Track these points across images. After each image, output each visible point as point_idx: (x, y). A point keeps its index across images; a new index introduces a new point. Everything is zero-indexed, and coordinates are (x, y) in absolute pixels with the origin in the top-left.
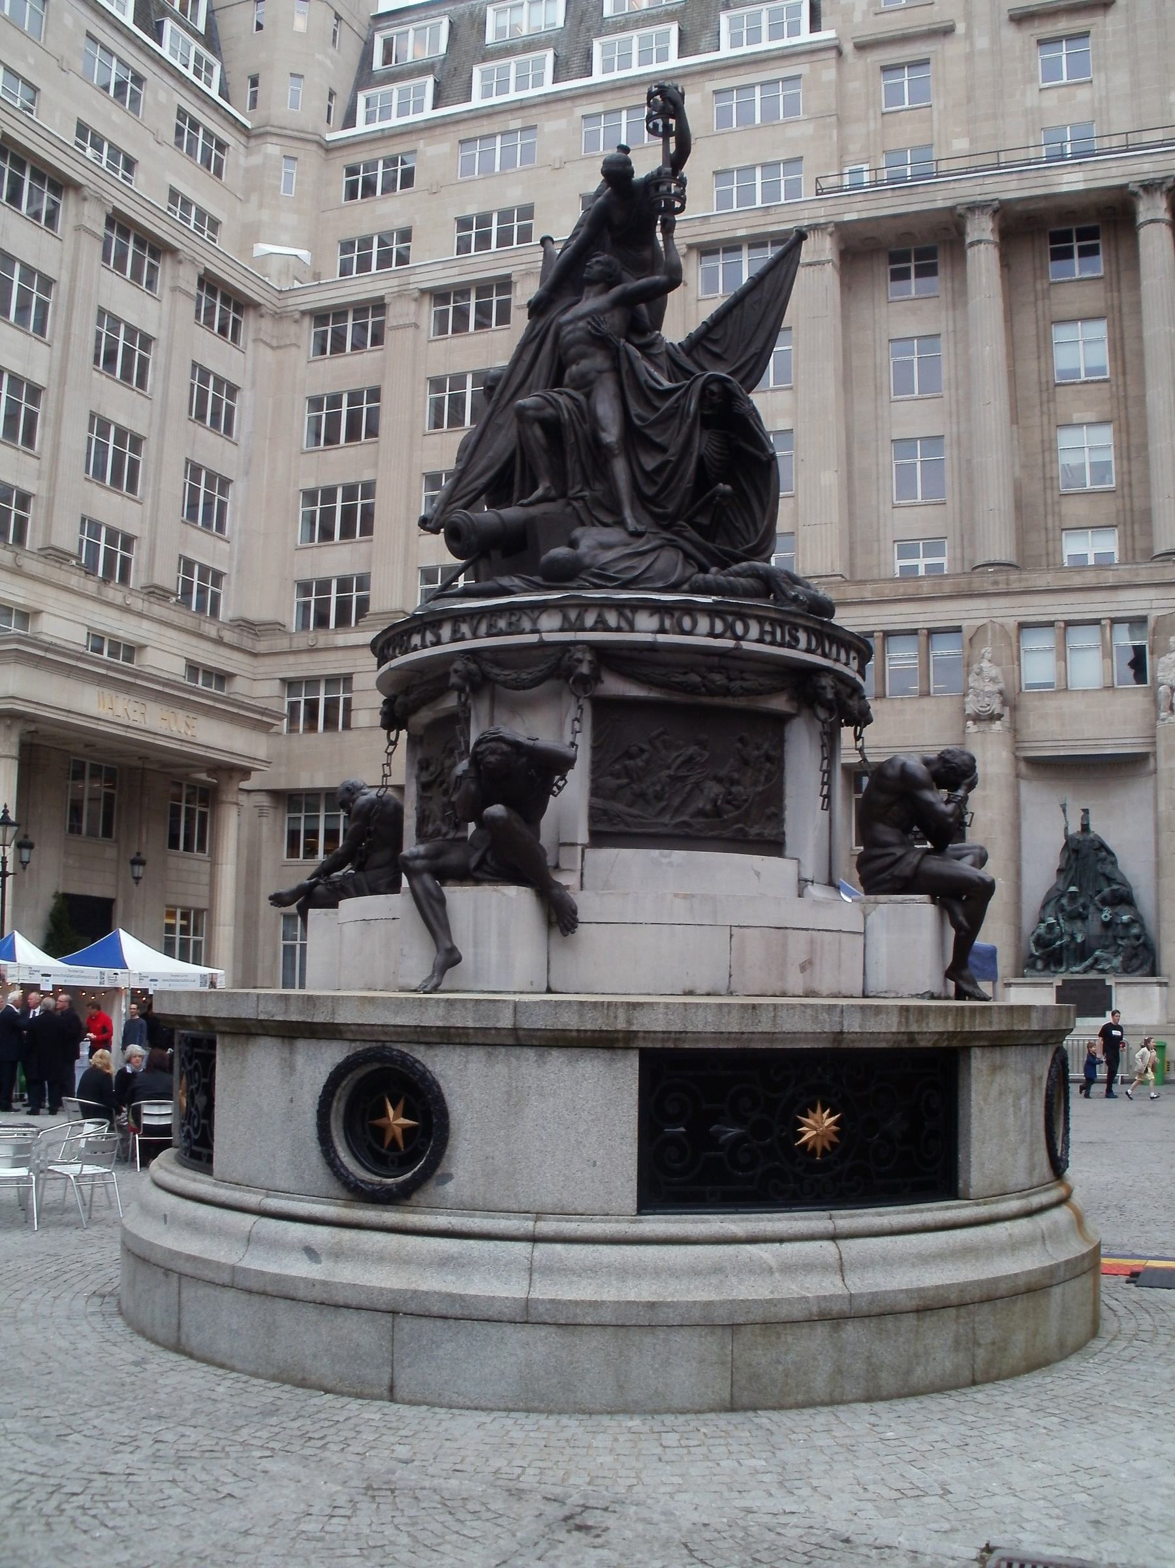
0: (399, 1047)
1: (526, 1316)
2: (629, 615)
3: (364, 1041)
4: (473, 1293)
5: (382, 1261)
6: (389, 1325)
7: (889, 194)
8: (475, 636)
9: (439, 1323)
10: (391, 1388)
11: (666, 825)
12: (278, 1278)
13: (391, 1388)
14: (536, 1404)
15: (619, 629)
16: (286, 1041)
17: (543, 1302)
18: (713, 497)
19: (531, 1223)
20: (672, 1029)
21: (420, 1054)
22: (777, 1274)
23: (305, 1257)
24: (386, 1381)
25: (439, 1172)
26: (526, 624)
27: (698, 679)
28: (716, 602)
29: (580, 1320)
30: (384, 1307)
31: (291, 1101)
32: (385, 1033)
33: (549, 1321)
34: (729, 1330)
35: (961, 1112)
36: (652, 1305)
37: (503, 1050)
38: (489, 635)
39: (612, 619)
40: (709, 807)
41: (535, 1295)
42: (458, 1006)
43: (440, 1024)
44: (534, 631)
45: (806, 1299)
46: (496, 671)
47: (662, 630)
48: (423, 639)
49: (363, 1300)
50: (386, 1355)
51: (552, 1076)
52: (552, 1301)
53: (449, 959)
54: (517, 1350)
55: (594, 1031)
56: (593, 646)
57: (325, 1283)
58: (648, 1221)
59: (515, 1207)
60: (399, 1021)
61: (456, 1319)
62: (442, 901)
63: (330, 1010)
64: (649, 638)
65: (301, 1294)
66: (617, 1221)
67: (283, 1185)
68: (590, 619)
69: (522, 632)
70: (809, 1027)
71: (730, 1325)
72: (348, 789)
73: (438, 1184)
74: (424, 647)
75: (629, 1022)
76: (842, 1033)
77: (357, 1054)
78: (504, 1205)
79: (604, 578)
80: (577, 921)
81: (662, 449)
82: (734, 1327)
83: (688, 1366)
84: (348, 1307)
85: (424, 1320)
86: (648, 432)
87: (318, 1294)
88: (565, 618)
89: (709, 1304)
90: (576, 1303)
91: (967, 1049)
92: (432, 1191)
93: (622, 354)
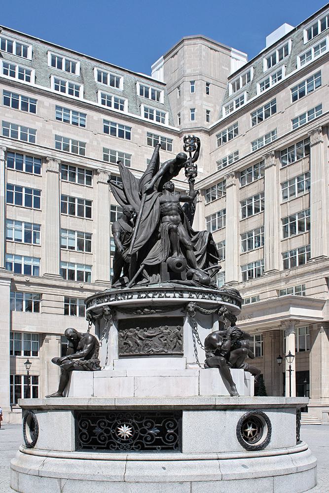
48: (174, 295)
74: (174, 297)
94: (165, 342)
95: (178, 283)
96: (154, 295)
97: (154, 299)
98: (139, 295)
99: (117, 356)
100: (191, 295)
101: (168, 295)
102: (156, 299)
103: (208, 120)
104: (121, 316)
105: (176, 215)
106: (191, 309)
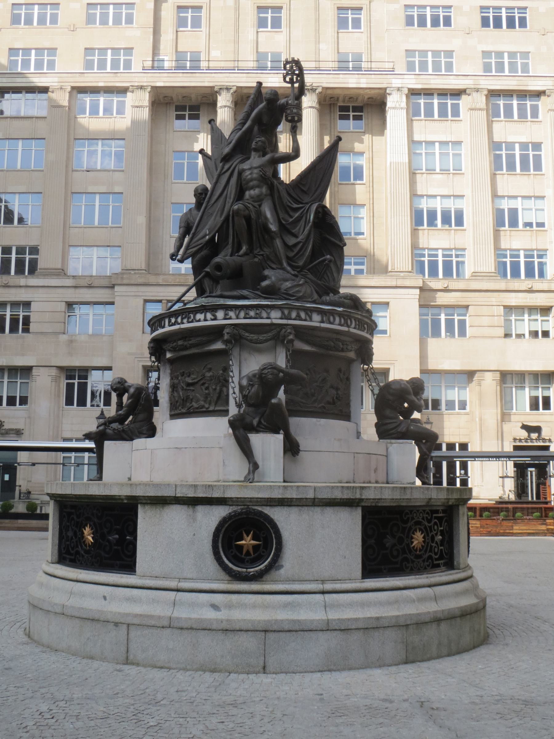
0: (256, 508)
1: (328, 628)
2: (310, 314)
3: (238, 505)
4: (304, 618)
5: (252, 607)
6: (263, 637)
7: (181, 75)
8: (237, 318)
9: (288, 634)
10: (264, 668)
11: (315, 407)
12: (200, 621)
13: (264, 668)
14: (332, 667)
15: (305, 320)
16: (190, 506)
17: (335, 620)
18: (325, 260)
19: (321, 586)
20: (377, 497)
21: (267, 510)
22: (416, 603)
23: (211, 609)
24: (262, 663)
25: (277, 565)
26: (264, 315)
27: (332, 344)
28: (344, 311)
29: (350, 627)
30: (261, 629)
31: (194, 535)
32: (251, 501)
33: (337, 628)
34: (405, 627)
35: (454, 533)
36: (378, 619)
37: (306, 508)
38: (245, 318)
39: (303, 315)
40: (331, 400)
41: (330, 617)
42: (289, 488)
43: (280, 497)
44: (268, 318)
45: (429, 612)
46: (247, 334)
47: (322, 322)
48: (205, 317)
49: (250, 627)
50: (262, 651)
51: (327, 519)
52: (339, 619)
53: (255, 466)
54: (323, 644)
55: (346, 499)
56: (294, 327)
57: (228, 620)
58: (367, 582)
59: (313, 579)
60: (260, 496)
61: (296, 631)
62: (248, 440)
63: (222, 491)
64: (317, 324)
65: (214, 627)
66: (355, 582)
67: (189, 576)
68: (294, 314)
69: (262, 318)
70: (422, 497)
71: (405, 626)
72: (119, 382)
73: (276, 570)
74: (205, 320)
75: (361, 495)
76: (430, 499)
77: (235, 511)
78: (307, 578)
79: (287, 295)
80: (299, 450)
81: (296, 236)
82: (407, 626)
83: (388, 643)
84: (241, 630)
85: (281, 633)
86: (288, 227)
87: (224, 625)
88: (283, 313)
89: (398, 616)
90: (349, 620)
91: (458, 506)
92: (274, 574)
93: (275, 188)
94: (207, 391)
96: (182, 319)
97: (183, 326)
102: (186, 325)
105: (258, 186)
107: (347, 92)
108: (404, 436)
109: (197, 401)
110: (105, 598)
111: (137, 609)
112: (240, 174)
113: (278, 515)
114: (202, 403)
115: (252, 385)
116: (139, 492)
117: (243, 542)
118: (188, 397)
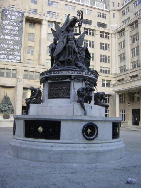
24: (96, 161)
44: (83, 74)
56: (89, 78)
69: (81, 74)
74: (66, 73)
88: (86, 73)
95: (69, 67)
97: (59, 74)
98: (54, 73)
99: (47, 98)
100: (72, 72)
101: (64, 72)
102: (60, 74)
103: (119, 6)
104: (49, 81)
106: (73, 78)
107: (33, 19)
108: (102, 105)
109: (60, 94)
110: (52, 146)
111: (63, 149)
112: (67, 36)
113: (97, 124)
114: (62, 95)
115: (83, 91)
116: (61, 118)
117: (88, 131)
118: (57, 93)
